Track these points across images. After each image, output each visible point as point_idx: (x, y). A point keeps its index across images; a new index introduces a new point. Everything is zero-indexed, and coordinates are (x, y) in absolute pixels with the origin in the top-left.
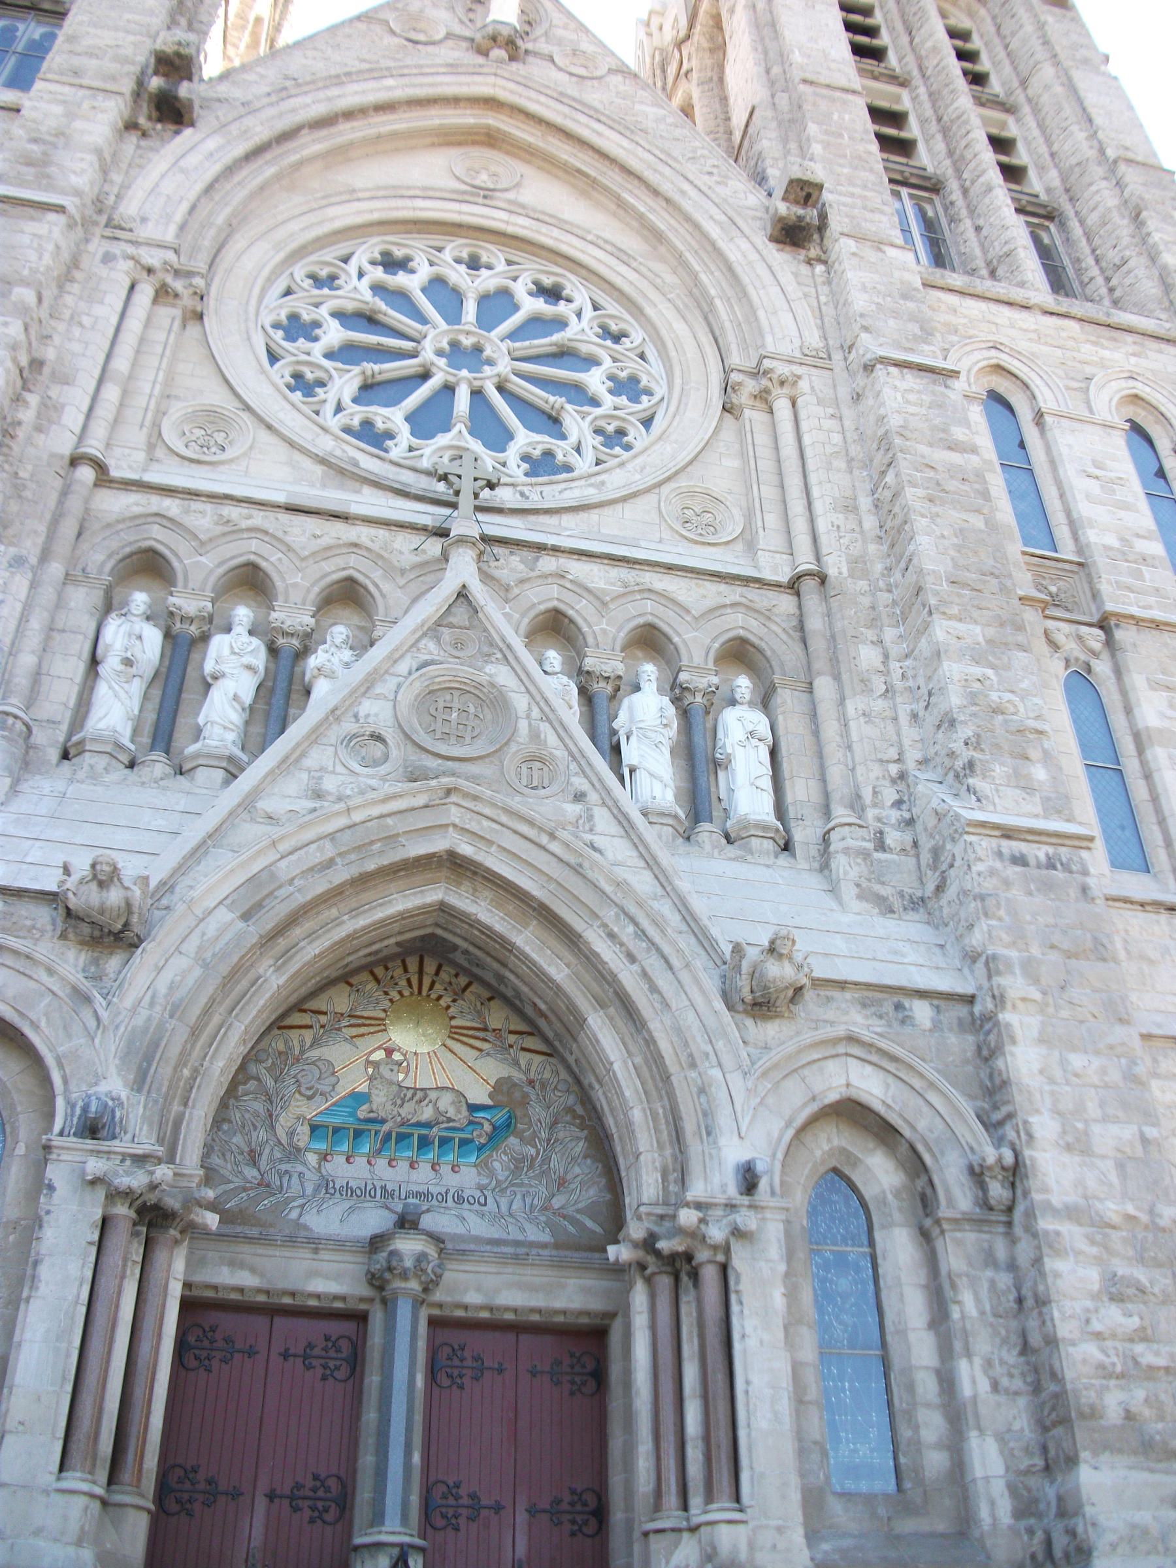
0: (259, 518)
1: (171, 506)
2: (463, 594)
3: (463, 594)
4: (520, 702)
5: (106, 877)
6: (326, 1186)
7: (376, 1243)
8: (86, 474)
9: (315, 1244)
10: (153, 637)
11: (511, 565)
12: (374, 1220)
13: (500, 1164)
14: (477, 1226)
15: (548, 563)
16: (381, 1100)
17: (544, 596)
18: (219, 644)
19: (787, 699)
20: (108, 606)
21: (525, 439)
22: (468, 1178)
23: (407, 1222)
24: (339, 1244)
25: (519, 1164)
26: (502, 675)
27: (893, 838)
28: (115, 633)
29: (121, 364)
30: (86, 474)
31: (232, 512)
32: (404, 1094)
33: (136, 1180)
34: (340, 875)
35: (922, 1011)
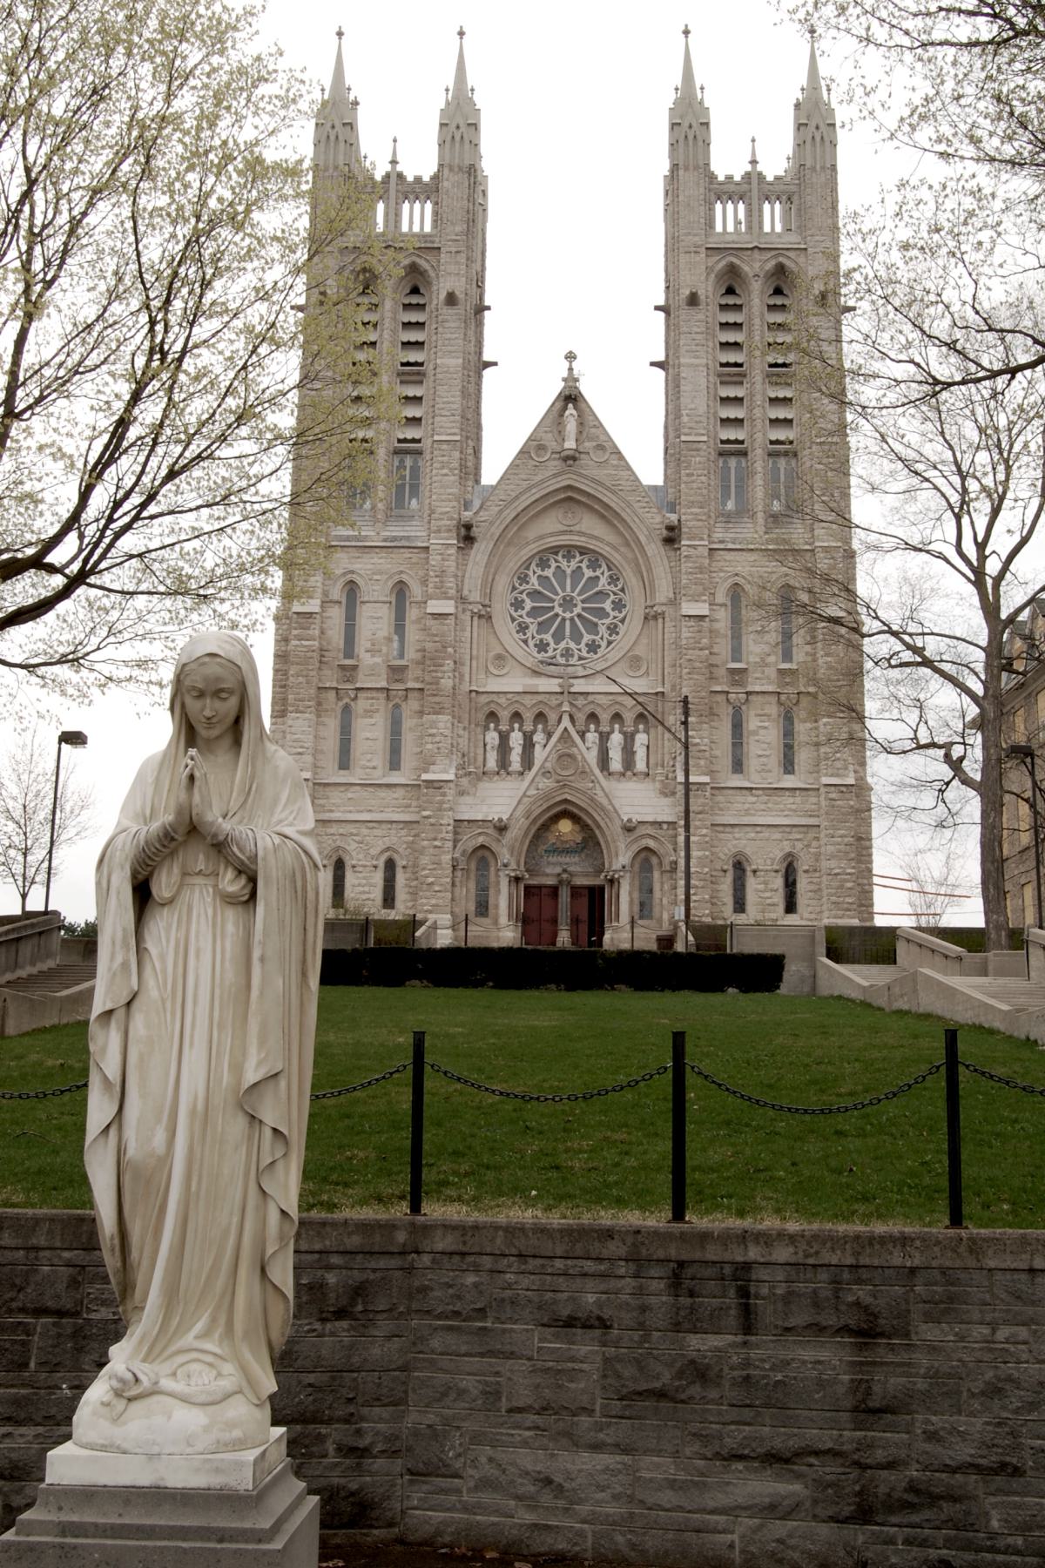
0: (517, 698)
1: (494, 698)
2: (566, 729)
3: (566, 729)
4: (579, 757)
5: (500, 820)
6: (549, 863)
7: (559, 875)
8: (474, 694)
9: (547, 875)
10: (496, 735)
11: (580, 702)
12: (558, 870)
13: (583, 855)
14: (579, 869)
15: (590, 698)
16: (558, 845)
17: (588, 710)
18: (513, 735)
19: (652, 731)
20: (486, 728)
21: (587, 638)
22: (576, 859)
23: (565, 871)
24: (552, 875)
25: (587, 855)
26: (575, 750)
27: (670, 775)
28: (488, 739)
29: (475, 653)
30: (474, 694)
31: (510, 696)
32: (563, 842)
33: (513, 874)
34: (545, 807)
35: (665, 826)
